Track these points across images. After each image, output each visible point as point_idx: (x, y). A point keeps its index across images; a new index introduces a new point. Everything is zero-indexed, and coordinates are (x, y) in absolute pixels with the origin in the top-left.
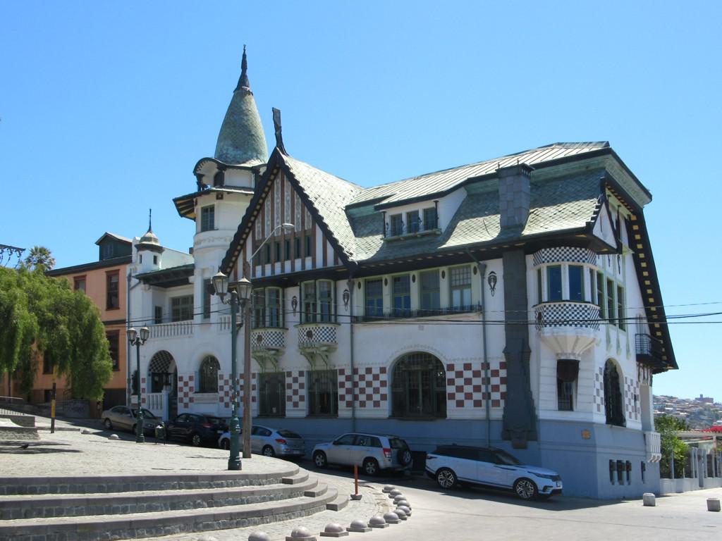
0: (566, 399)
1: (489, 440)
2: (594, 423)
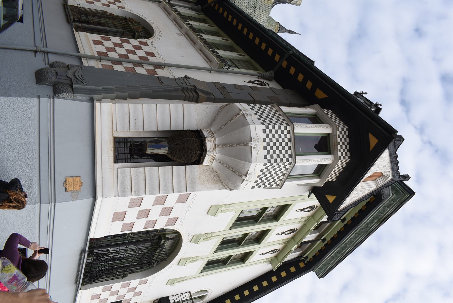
0: (131, 150)
1: (48, 53)
2: (95, 197)
